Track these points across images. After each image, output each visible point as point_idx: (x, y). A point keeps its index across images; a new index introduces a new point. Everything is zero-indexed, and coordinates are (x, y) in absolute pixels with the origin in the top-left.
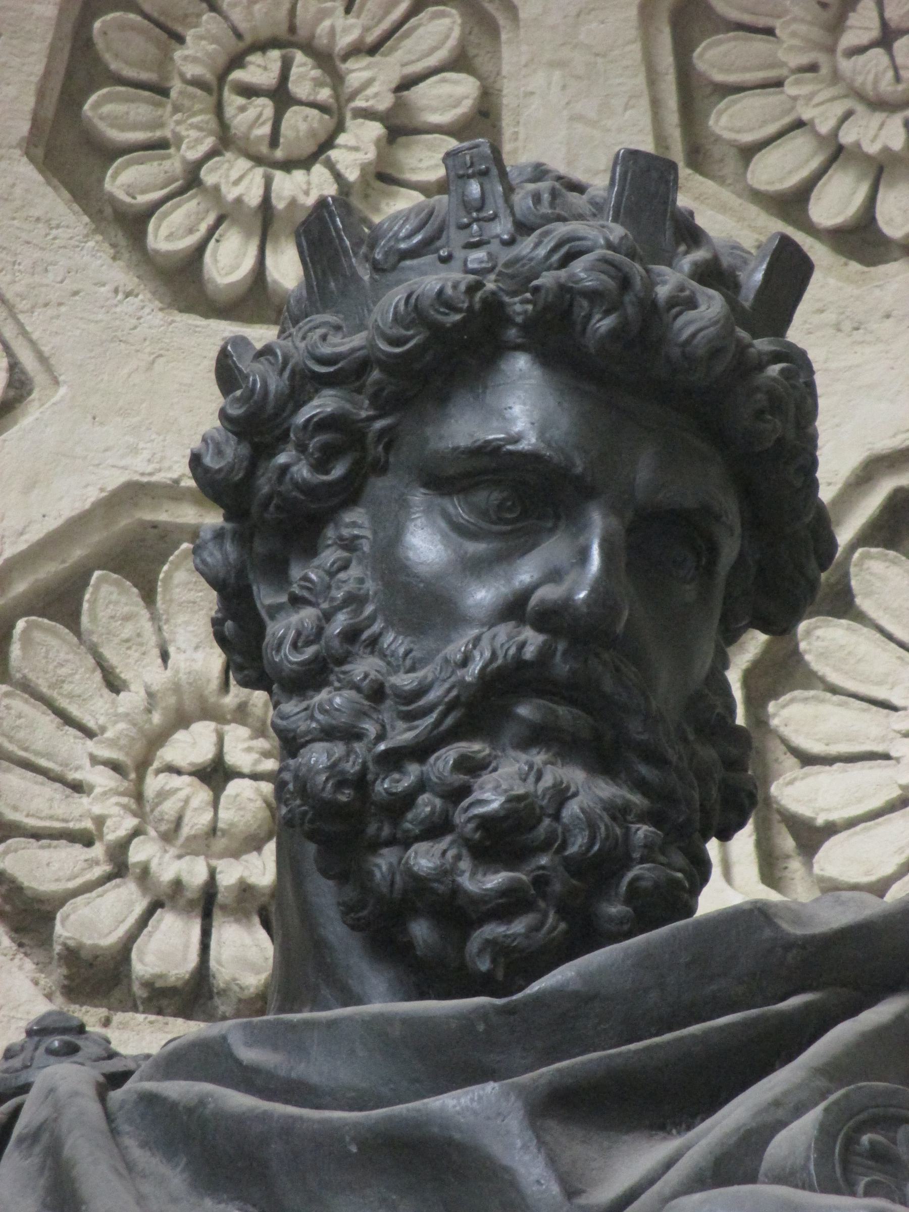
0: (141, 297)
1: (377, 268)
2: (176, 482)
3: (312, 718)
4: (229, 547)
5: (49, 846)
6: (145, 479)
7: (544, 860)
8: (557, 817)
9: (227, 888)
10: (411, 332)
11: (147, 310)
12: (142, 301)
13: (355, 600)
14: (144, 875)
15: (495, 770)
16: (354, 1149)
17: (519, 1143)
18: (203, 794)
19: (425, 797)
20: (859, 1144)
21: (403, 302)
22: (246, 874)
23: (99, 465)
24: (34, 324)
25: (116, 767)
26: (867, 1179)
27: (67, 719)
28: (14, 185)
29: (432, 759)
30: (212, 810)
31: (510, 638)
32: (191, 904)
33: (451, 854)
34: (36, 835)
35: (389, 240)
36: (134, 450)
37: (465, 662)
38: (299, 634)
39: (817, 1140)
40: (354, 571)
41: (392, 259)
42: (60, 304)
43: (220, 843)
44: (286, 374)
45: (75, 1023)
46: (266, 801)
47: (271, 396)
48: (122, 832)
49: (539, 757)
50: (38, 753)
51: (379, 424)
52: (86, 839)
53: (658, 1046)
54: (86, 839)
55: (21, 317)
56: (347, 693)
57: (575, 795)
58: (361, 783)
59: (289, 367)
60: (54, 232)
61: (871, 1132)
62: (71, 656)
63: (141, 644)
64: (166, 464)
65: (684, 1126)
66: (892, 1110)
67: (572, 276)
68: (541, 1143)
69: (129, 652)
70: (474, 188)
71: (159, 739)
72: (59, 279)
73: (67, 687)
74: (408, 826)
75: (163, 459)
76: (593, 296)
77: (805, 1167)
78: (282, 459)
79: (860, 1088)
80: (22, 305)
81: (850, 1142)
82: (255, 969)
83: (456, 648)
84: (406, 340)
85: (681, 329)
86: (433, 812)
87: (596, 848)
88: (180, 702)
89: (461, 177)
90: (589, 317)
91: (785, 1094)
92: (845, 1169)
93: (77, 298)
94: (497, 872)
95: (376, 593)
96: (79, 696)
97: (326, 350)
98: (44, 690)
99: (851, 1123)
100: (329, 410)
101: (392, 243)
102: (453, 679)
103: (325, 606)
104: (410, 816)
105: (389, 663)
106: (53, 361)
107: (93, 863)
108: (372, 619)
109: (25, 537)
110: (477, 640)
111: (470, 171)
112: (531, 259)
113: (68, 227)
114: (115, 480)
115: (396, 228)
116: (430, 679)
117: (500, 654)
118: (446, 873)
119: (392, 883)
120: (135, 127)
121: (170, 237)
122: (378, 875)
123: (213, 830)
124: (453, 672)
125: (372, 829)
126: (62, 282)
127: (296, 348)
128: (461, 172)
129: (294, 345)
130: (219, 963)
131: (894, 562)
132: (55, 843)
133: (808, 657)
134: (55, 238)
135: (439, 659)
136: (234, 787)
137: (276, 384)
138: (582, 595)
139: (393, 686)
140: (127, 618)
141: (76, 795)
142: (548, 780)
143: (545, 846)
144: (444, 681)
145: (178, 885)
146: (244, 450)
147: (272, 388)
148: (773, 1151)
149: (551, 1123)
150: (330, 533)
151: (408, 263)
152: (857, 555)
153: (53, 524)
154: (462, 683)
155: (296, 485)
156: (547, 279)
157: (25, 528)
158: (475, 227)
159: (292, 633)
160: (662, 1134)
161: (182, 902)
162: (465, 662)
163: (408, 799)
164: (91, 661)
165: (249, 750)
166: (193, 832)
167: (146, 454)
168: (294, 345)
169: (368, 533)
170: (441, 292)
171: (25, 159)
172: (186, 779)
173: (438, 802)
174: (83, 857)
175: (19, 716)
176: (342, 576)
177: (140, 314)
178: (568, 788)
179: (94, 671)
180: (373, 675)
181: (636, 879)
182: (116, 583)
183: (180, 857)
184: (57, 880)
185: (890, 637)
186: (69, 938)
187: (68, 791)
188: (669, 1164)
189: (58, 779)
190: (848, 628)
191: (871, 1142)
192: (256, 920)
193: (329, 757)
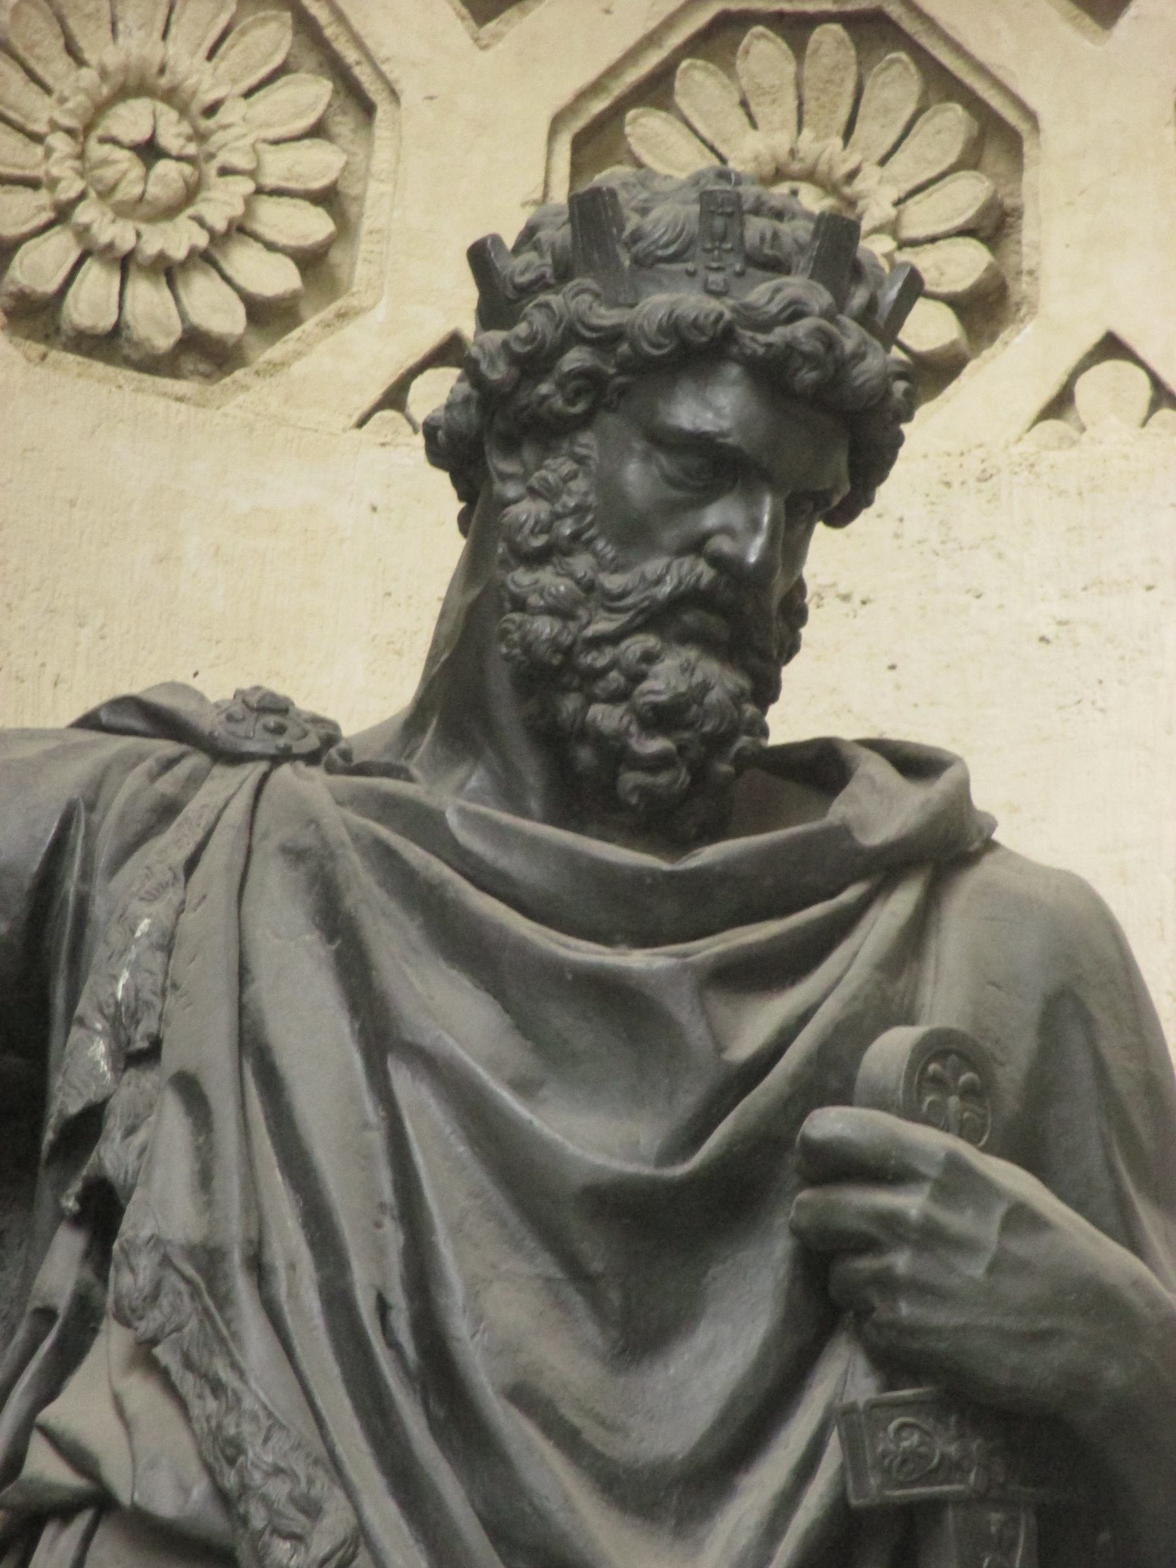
1: (637, 261)
3: (542, 596)
4: (473, 410)
7: (687, 735)
8: (701, 704)
9: (150, 257)
10: (667, 341)
13: (580, 510)
14: (83, 232)
15: (663, 661)
16: (570, 977)
17: (689, 1008)
18: (137, 170)
19: (614, 674)
21: (666, 317)
25: (70, 132)
26: (929, 1099)
27: (32, 76)
29: (624, 645)
30: (142, 183)
31: (692, 569)
32: (115, 259)
33: (626, 720)
35: (649, 246)
37: (659, 581)
38: (536, 523)
40: (580, 485)
41: (649, 261)
43: (144, 209)
44: (560, 331)
45: (283, 706)
47: (547, 345)
48: (73, 193)
49: (691, 653)
50: (10, 107)
51: (621, 380)
52: (33, 184)
56: (569, 583)
57: (713, 688)
58: (568, 652)
59: (563, 325)
62: (43, 25)
67: (795, 338)
68: (704, 1012)
70: (719, 223)
71: (101, 108)
73: (37, 51)
74: (597, 691)
76: (808, 357)
77: (895, 1091)
78: (544, 388)
83: (654, 566)
84: (664, 346)
85: (856, 378)
86: (618, 688)
87: (723, 729)
88: (125, 81)
89: (713, 212)
90: (799, 369)
92: (919, 1093)
94: (653, 737)
95: (596, 508)
97: (596, 321)
98: (21, 52)
100: (588, 364)
101: (652, 248)
102: (648, 593)
103: (558, 508)
104: (601, 684)
105: (599, 564)
107: (41, 208)
108: (591, 525)
110: (668, 567)
111: (720, 210)
112: (766, 313)
115: (657, 236)
116: (630, 586)
117: (685, 582)
118: (622, 735)
119: (575, 720)
122: (565, 715)
123: (141, 198)
124: (646, 589)
125: (566, 680)
127: (568, 308)
128: (712, 208)
129: (566, 304)
131: (713, 74)
133: (631, 140)
135: (637, 570)
136: (164, 167)
137: (551, 335)
138: (752, 558)
139: (602, 586)
142: (698, 677)
143: (689, 726)
144: (641, 592)
145: (110, 246)
146: (515, 372)
147: (549, 338)
149: (710, 994)
150: (565, 445)
151: (662, 266)
152: (685, 64)
154: (653, 599)
155: (551, 411)
156: (778, 335)
158: (716, 252)
159: (531, 522)
162: (659, 581)
163: (603, 672)
164: (58, 29)
165: (179, 135)
166: (126, 198)
168: (566, 304)
169: (594, 455)
170: (696, 319)
173: (622, 680)
174: (35, 204)
176: (573, 485)
178: (710, 684)
180: (590, 574)
181: (742, 749)
183: (114, 221)
184: (16, 224)
185: (695, 132)
187: (27, 140)
189: (20, 129)
190: (665, 120)
192: (163, 280)
193: (552, 630)
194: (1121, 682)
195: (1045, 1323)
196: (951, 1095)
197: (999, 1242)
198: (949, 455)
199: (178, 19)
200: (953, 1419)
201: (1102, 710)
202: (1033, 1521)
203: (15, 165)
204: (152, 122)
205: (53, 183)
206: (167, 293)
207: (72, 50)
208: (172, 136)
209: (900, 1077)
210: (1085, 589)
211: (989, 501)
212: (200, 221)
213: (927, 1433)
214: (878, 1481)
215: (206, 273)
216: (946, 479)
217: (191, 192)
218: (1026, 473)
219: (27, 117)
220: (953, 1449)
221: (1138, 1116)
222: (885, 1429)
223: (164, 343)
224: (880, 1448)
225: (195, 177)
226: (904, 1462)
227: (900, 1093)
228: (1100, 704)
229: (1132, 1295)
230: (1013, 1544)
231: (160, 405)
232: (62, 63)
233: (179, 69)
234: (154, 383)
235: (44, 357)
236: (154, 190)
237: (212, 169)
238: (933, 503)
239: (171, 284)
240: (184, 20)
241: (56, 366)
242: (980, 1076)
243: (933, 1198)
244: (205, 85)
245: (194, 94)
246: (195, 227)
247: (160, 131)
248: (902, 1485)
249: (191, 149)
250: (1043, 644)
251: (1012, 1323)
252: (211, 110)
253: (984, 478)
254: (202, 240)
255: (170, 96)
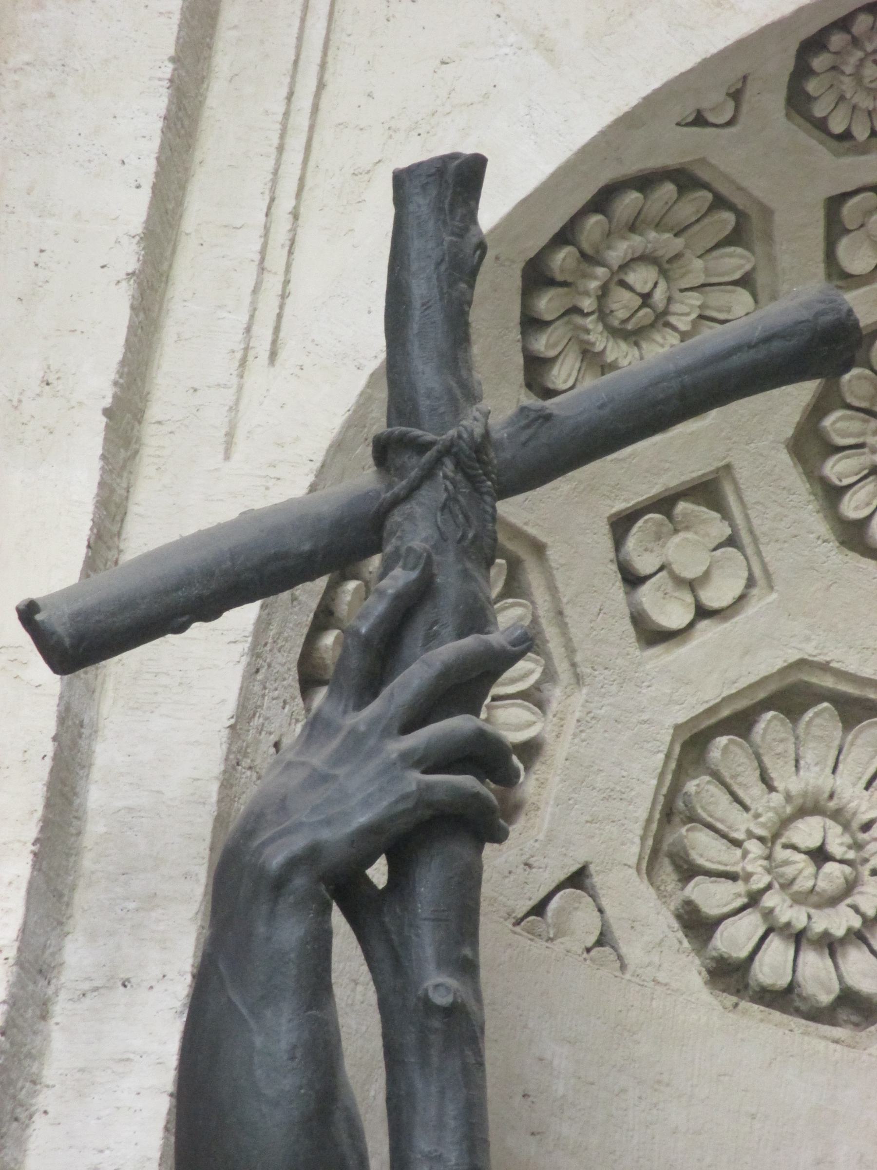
0: (831, 544)
2: (828, 662)
5: (716, 882)
6: (811, 658)
9: (817, 933)
11: (834, 553)
12: (832, 547)
14: (768, 914)
18: (811, 869)
22: (829, 926)
23: (786, 645)
24: (769, 553)
25: (761, 839)
27: (737, 800)
28: (775, 466)
34: (709, 873)
36: (808, 639)
42: (785, 542)
43: (814, 899)
46: (846, 879)
48: (761, 885)
50: (718, 820)
52: (733, 877)
54: (733, 877)
55: (761, 546)
60: (791, 497)
62: (746, 760)
63: (785, 757)
64: (825, 651)
69: (778, 761)
71: (785, 823)
72: (788, 526)
73: (740, 779)
75: (824, 647)
80: (763, 540)
82: (829, 992)
88: (804, 803)
93: (795, 539)
96: (745, 785)
98: (728, 780)
106: (773, 577)
107: (739, 895)
109: (736, 685)
113: (800, 495)
114: (794, 656)
120: (851, 435)
121: (857, 508)
123: (812, 890)
126: (789, 528)
130: (804, 979)
132: (719, 879)
134: (791, 501)
136: (830, 867)
140: (782, 741)
141: (733, 848)
145: (788, 925)
153: (753, 679)
157: (737, 679)
161: (787, 932)
164: (756, 764)
165: (842, 844)
166: (801, 889)
167: (814, 643)
171: (785, 451)
172: (803, 857)
174: (734, 891)
175: (712, 796)
177: (829, 554)
179: (756, 770)
182: (782, 721)
183: (791, 906)
186: (726, 953)
187: (729, 844)
189: (724, 836)
192: (827, 951)
199: (845, 759)
203: (720, 863)
204: (822, 834)
205: (748, 877)
206: (829, 962)
207: (765, 779)
208: (837, 845)
212: (856, 909)
215: (859, 948)
217: (850, 887)
219: (730, 827)
223: (825, 998)
225: (853, 876)
231: (821, 1045)
232: (758, 789)
233: (844, 796)
234: (817, 1029)
235: (736, 1005)
236: (822, 884)
237: (866, 870)
239: (833, 955)
240: (849, 760)
241: (745, 1012)
244: (863, 808)
245: (855, 814)
246: (851, 912)
247: (829, 840)
249: (851, 855)
252: (866, 827)
254: (856, 922)
255: (837, 815)
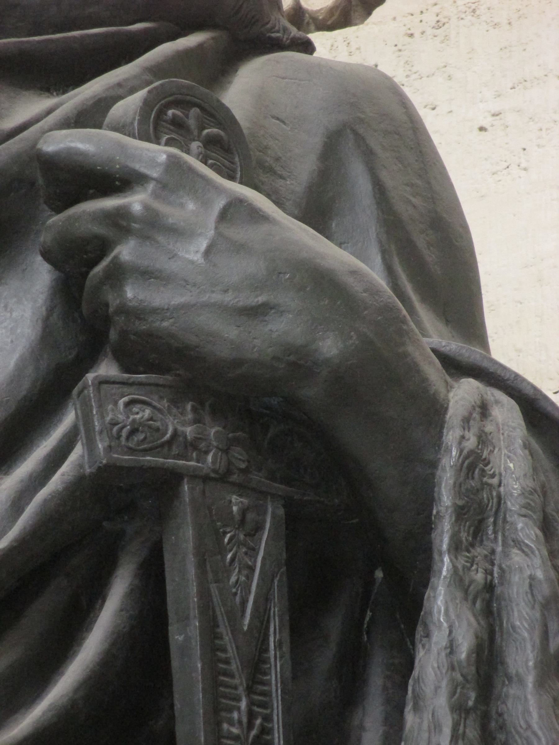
20: (166, 115)
26: (168, 136)
39: (141, 108)
53: (52, 41)
61: (174, 109)
65: (61, 91)
66: (188, 98)
79: (171, 81)
81: (161, 113)
91: (126, 80)
92: (155, 128)
99: (163, 102)
148: (113, 112)
160: (47, 94)
188: (49, 112)
191: (174, 114)
194: (539, 146)
195: (261, 299)
196: (194, 140)
197: (216, 228)
198: (412, 15)
200: (189, 407)
201: (525, 169)
202: (281, 512)
209: (135, 114)
210: (513, 88)
211: (442, 42)
213: (159, 410)
214: (106, 444)
216: (410, 32)
218: (469, 17)
220: (189, 431)
221: (421, 241)
222: (116, 403)
224: (108, 419)
226: (133, 432)
227: (136, 124)
228: (523, 165)
229: (350, 280)
230: (258, 528)
238: (400, 50)
242: (224, 129)
243: (156, 195)
248: (132, 451)
250: (483, 133)
251: (228, 298)
253: (439, 25)
